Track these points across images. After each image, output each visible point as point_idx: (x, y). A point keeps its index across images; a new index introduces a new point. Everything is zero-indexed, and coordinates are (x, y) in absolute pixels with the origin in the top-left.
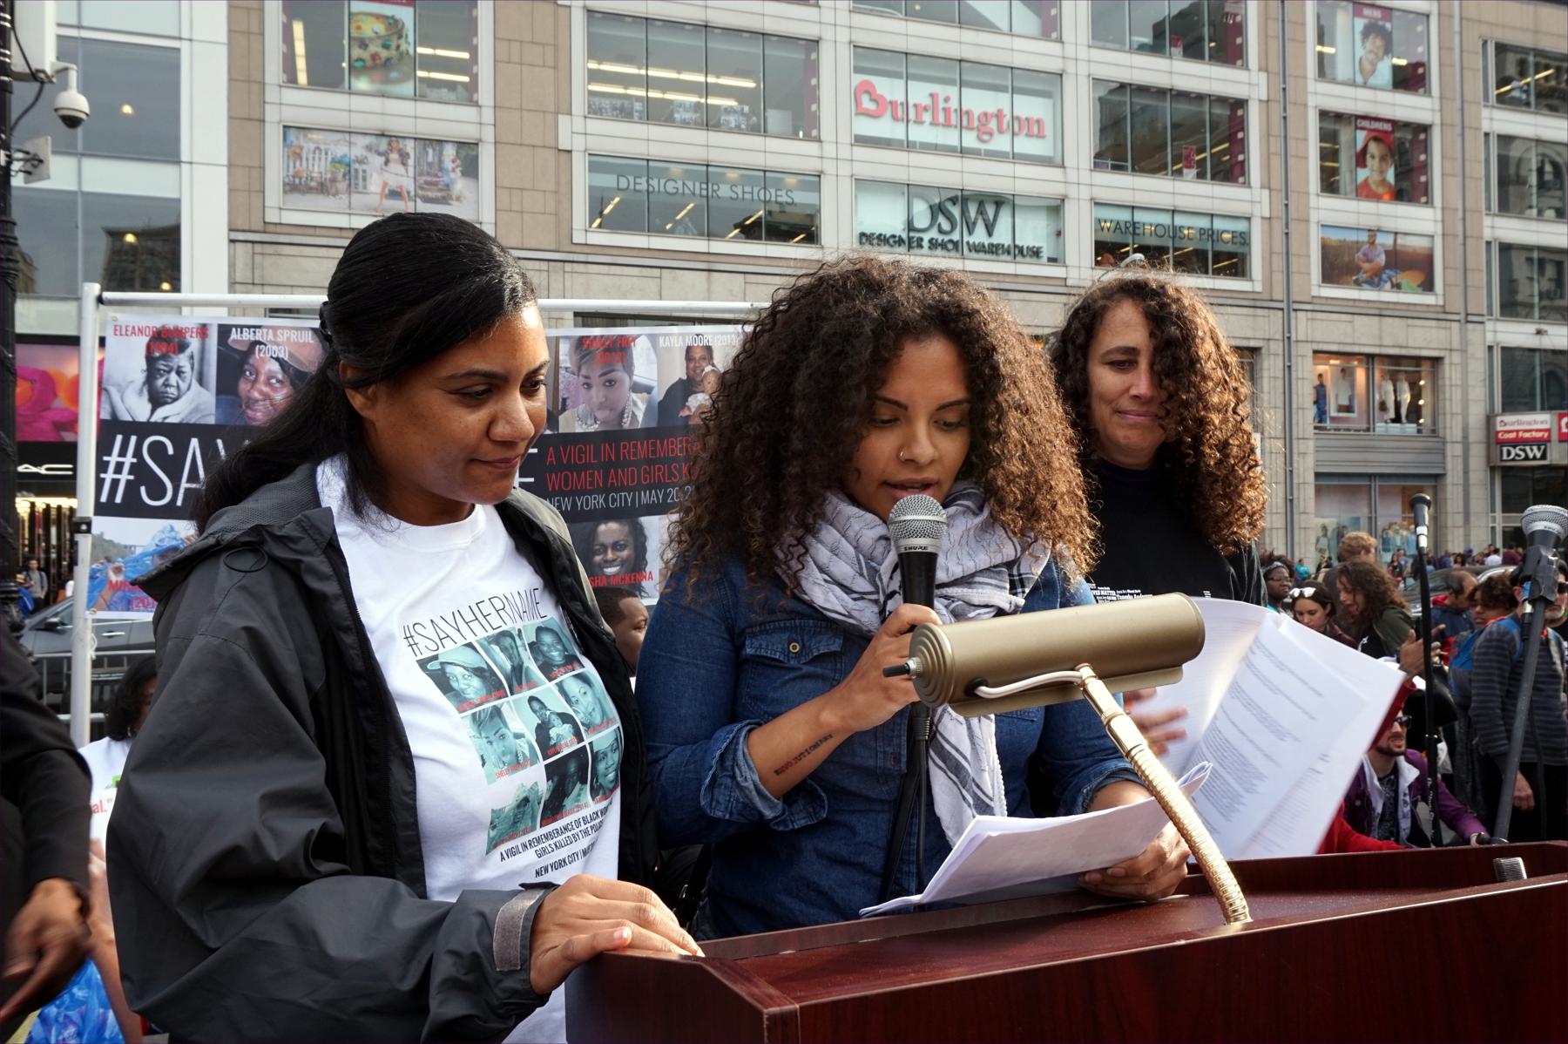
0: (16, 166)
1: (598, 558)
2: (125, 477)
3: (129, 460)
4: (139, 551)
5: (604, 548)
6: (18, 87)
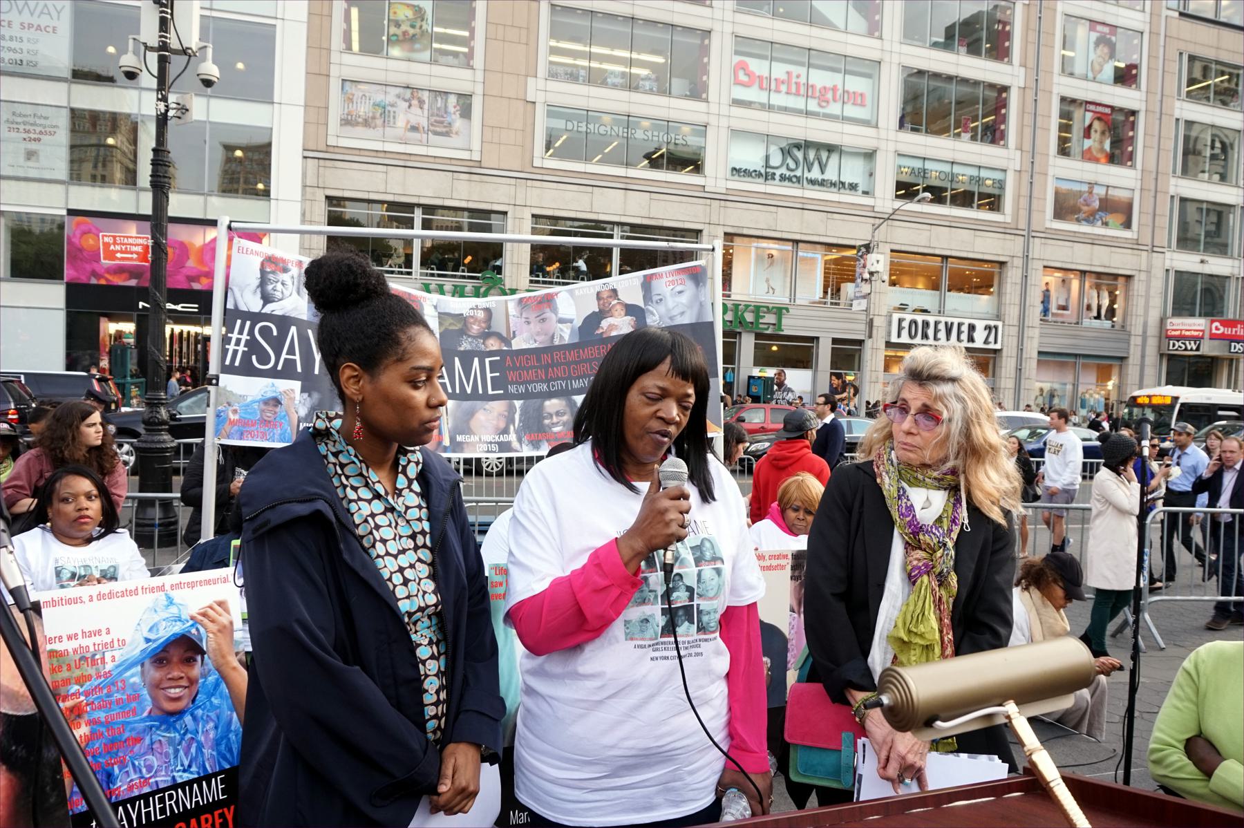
0: (171, 113)
1: (547, 422)
2: (242, 348)
3: (245, 337)
4: (249, 399)
5: (551, 416)
6: (174, 58)
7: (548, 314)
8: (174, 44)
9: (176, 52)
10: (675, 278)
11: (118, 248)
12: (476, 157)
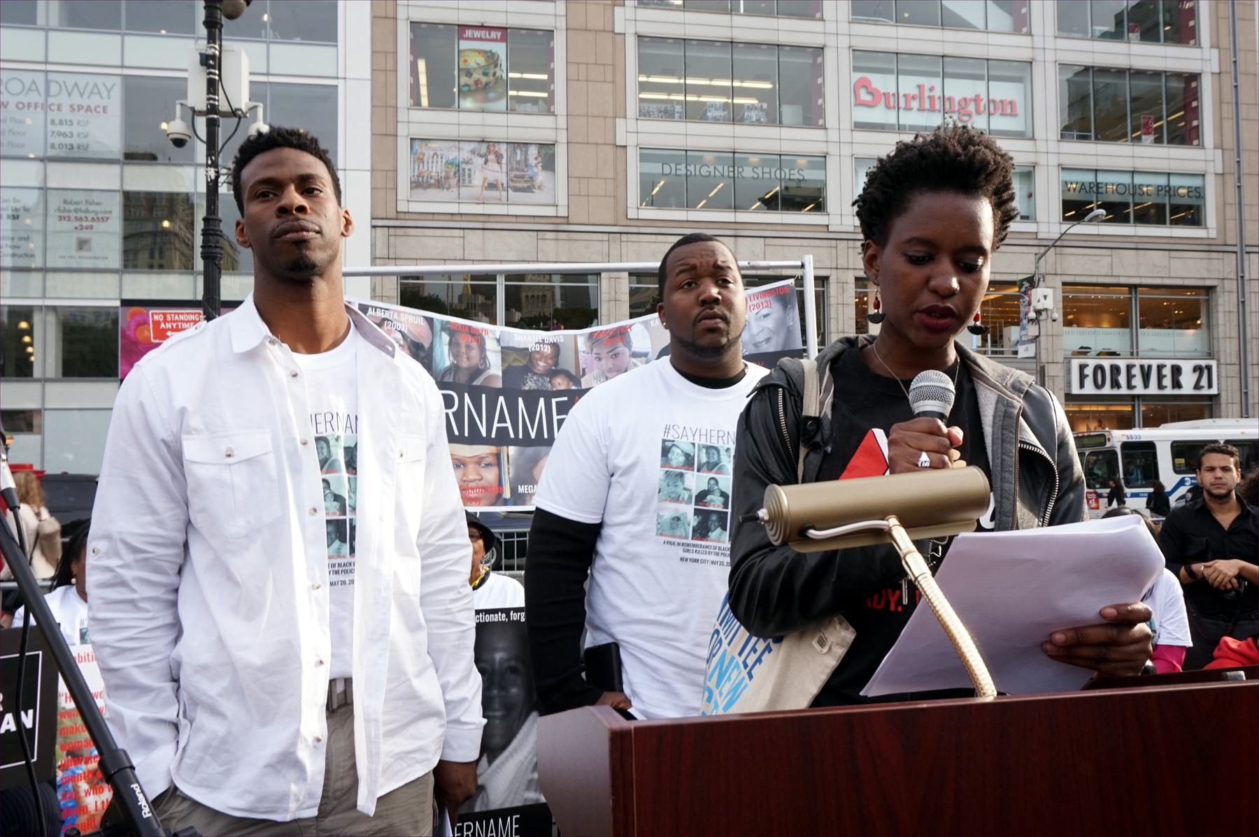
0: (222, 179)
7: (622, 348)
8: (223, 106)
9: (225, 115)
10: (760, 301)
11: (168, 325)
12: (563, 212)
